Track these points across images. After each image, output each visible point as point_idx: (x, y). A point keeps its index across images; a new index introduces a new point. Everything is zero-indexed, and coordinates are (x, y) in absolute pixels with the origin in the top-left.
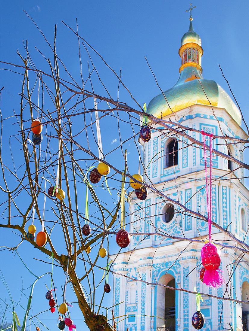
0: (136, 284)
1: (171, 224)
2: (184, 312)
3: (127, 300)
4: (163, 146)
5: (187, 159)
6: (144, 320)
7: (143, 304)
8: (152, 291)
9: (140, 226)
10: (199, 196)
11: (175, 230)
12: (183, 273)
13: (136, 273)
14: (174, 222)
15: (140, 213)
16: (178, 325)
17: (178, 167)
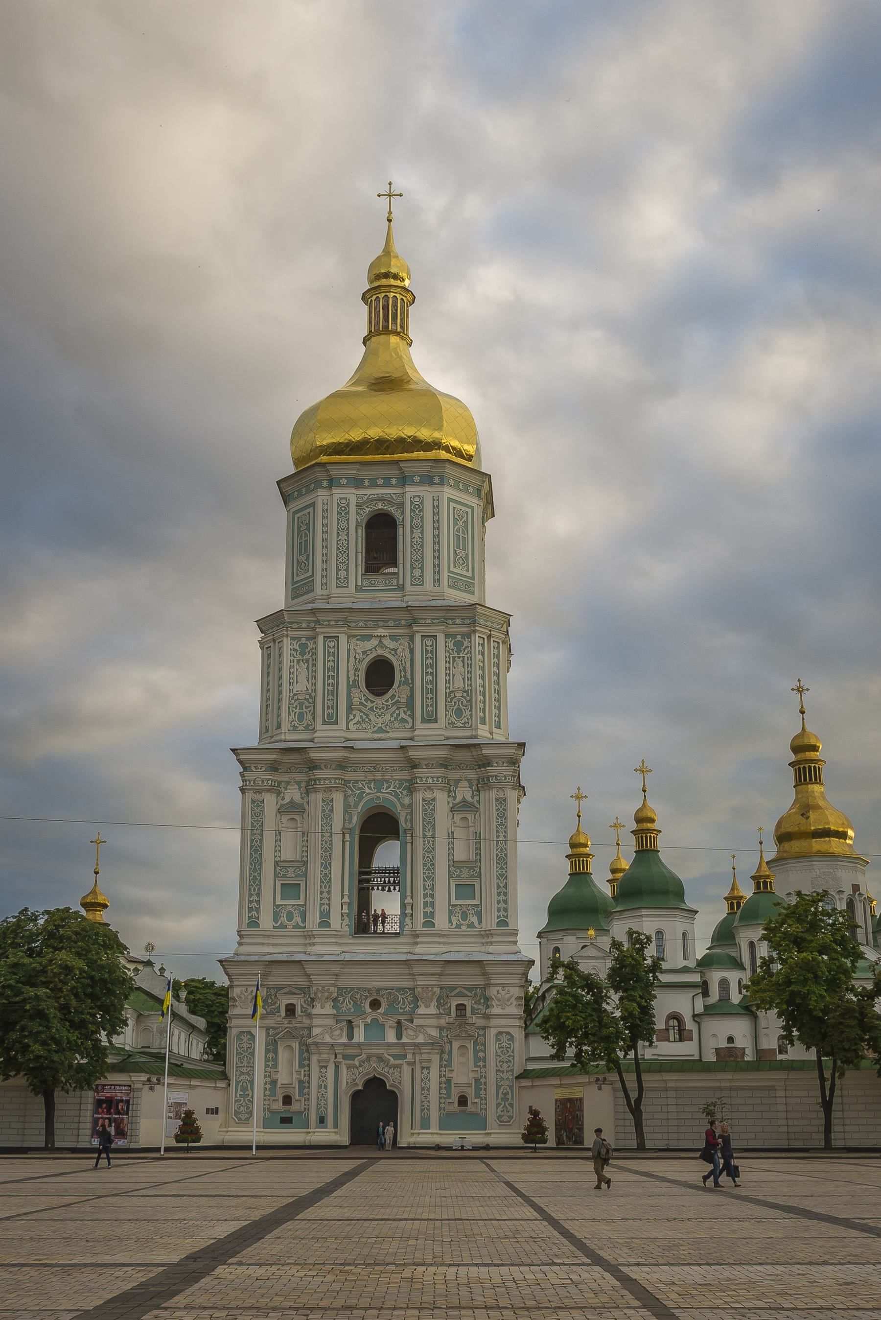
0: (303, 818)
1: (387, 701)
2: (425, 889)
3: (280, 851)
4: (359, 520)
5: (422, 568)
6: (329, 899)
7: (327, 865)
8: (344, 837)
9: (308, 690)
10: (450, 654)
11: (395, 715)
12: (423, 810)
13: (301, 794)
14: (393, 696)
15: (308, 660)
16: (406, 914)
17: (398, 579)
